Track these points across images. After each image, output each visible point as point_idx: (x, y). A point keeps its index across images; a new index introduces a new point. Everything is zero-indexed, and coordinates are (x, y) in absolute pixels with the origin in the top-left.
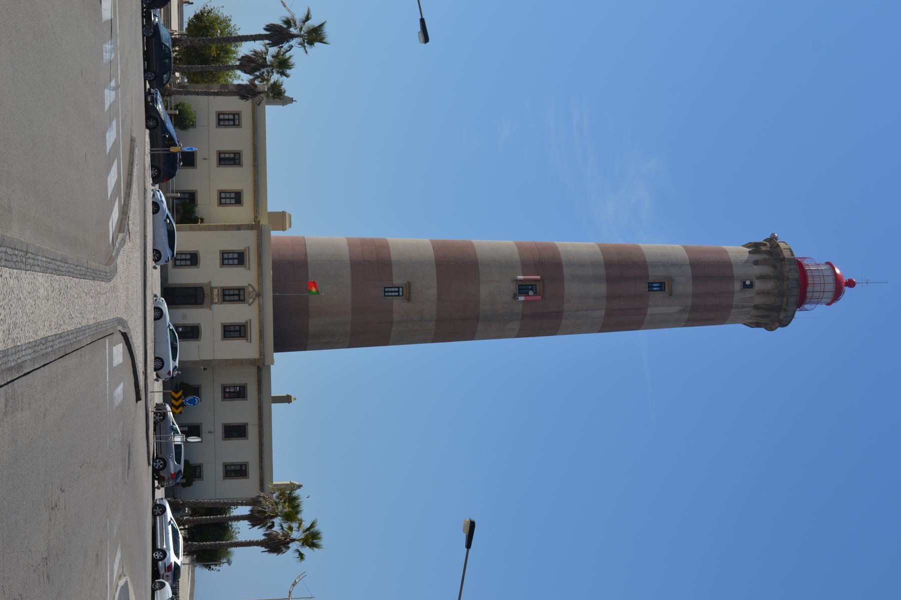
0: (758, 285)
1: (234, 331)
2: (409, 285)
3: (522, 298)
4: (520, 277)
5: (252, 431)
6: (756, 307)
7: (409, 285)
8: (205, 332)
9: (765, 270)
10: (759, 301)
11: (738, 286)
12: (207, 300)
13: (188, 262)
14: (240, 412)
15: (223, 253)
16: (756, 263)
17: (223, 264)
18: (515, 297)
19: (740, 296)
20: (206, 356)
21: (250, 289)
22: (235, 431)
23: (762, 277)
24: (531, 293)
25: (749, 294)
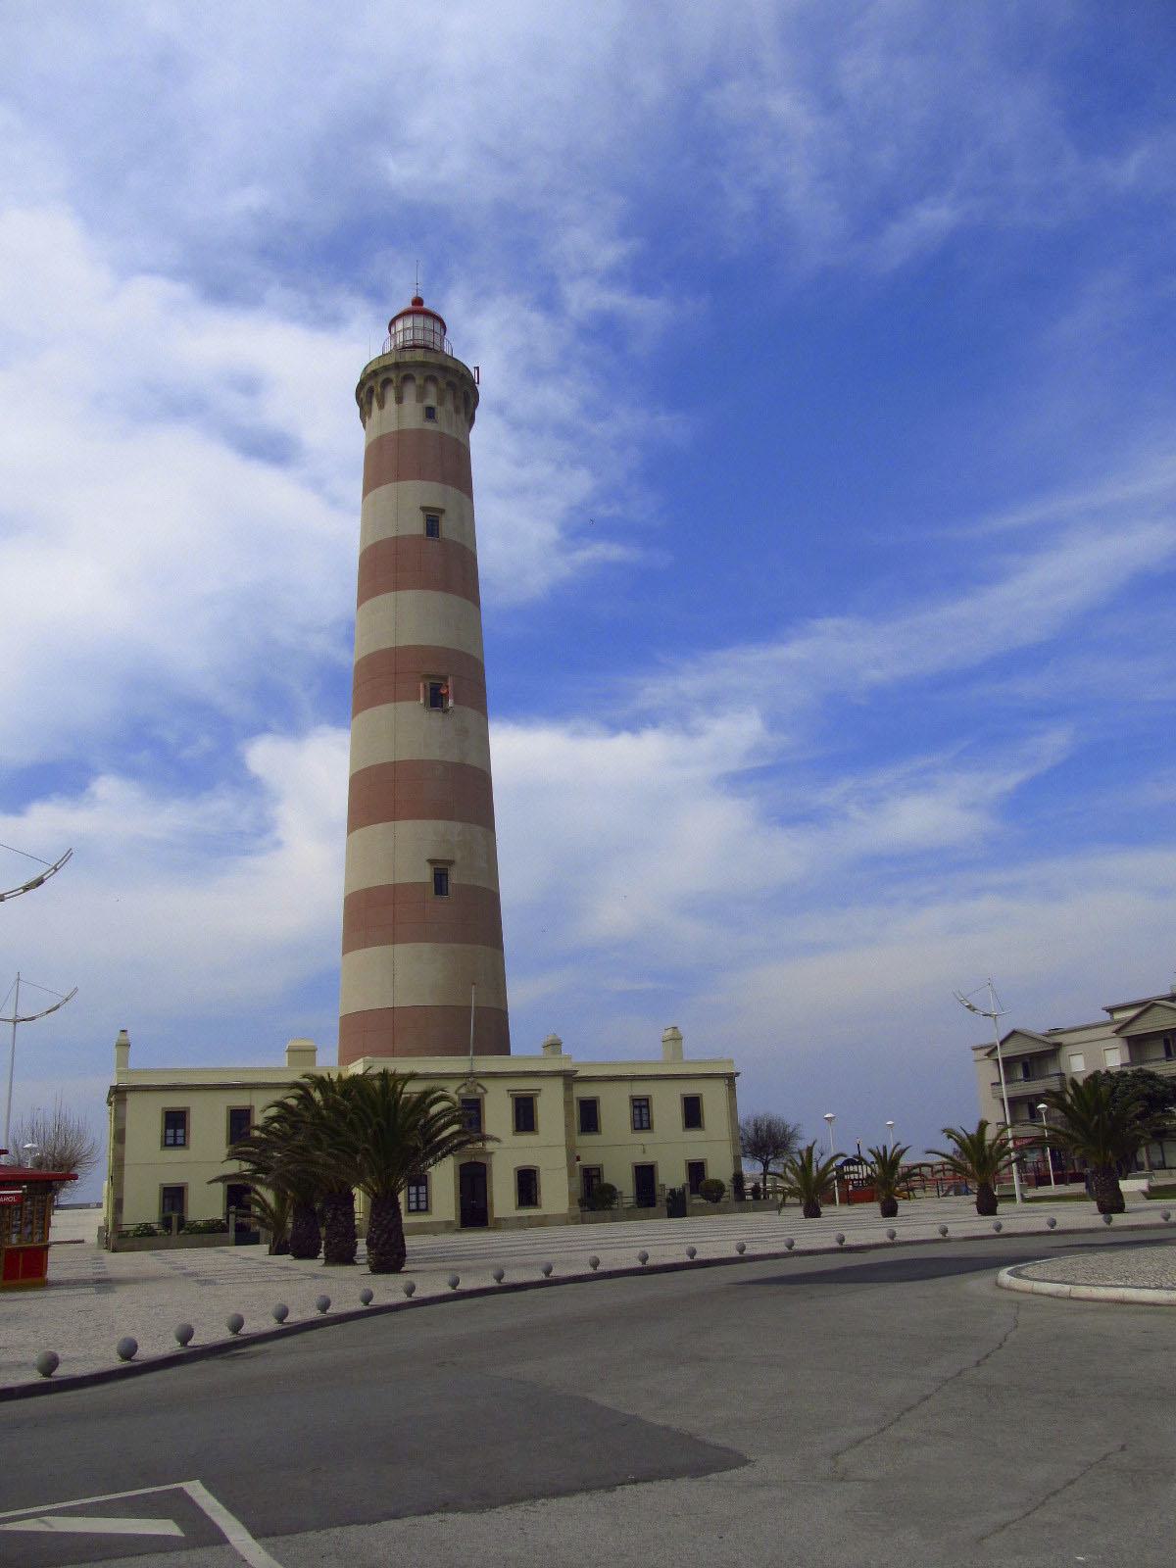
0: (431, 401)
1: (525, 1116)
2: (432, 862)
3: (451, 703)
4: (422, 701)
5: (640, 1089)
6: (457, 411)
7: (432, 862)
8: (527, 1161)
9: (410, 391)
10: (449, 406)
11: (430, 426)
12: (480, 1160)
13: (422, 1189)
14: (667, 1108)
15: (165, 1145)
16: (399, 400)
17: (184, 1145)
18: (446, 711)
19: (443, 425)
20: (561, 1157)
21: (463, 1091)
22: (641, 1113)
23: (421, 395)
24: (444, 691)
25: (440, 412)
